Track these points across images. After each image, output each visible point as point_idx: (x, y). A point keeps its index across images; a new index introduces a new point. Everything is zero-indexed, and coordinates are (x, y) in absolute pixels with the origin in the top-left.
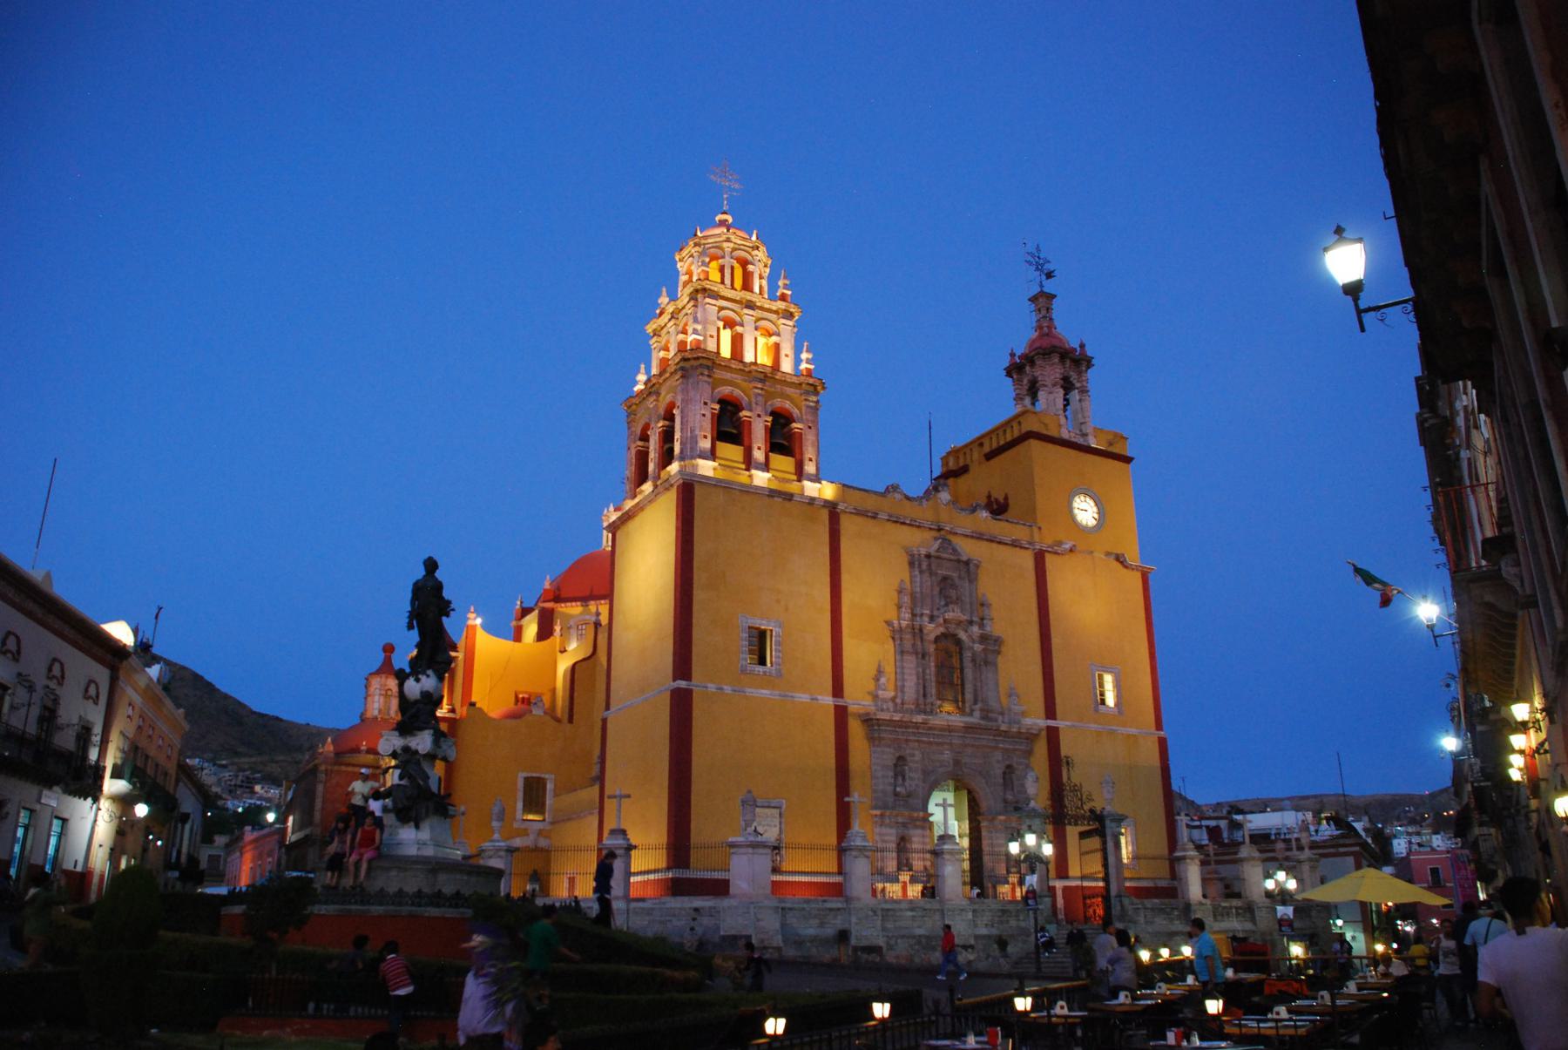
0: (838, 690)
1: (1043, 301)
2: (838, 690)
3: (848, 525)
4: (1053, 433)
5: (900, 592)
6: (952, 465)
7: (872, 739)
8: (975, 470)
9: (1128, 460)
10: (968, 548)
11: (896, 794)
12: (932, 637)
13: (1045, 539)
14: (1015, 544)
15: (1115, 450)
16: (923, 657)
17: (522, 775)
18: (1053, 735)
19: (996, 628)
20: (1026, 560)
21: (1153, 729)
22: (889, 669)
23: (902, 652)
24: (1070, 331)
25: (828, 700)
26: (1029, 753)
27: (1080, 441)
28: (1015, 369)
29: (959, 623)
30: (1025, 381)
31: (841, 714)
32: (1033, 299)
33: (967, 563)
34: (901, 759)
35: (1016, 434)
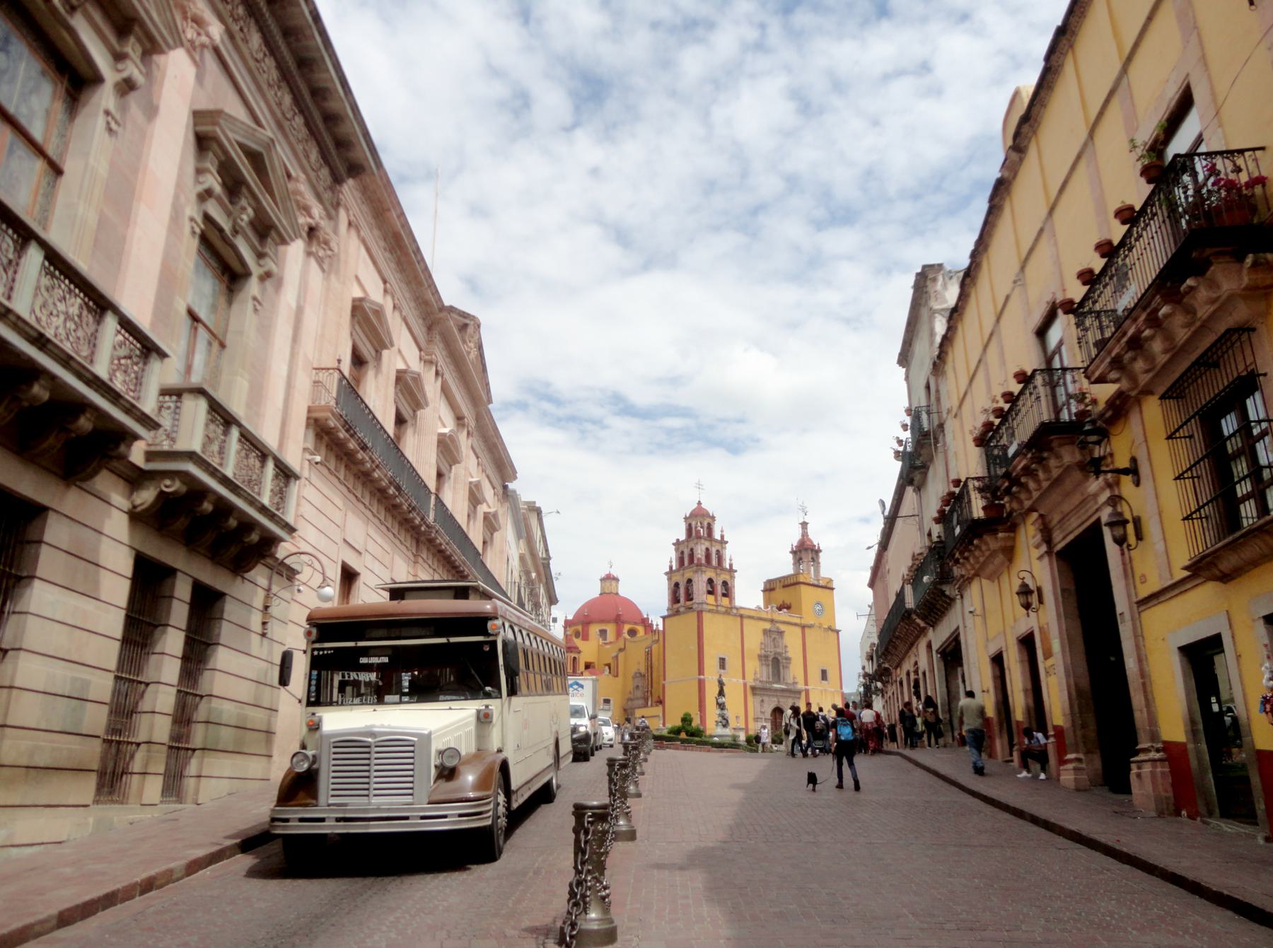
0: (744, 677)
1: (804, 525)
2: (744, 677)
3: (746, 621)
4: (808, 581)
5: (762, 643)
6: (768, 587)
7: (754, 694)
8: (777, 590)
9: (833, 589)
10: (782, 627)
11: (762, 712)
12: (770, 659)
13: (804, 622)
14: (796, 625)
15: (829, 585)
16: (768, 665)
17: (603, 698)
18: (807, 692)
19: (790, 655)
20: (798, 630)
21: (839, 689)
22: (758, 670)
23: (762, 664)
24: (815, 538)
25: (741, 681)
26: (799, 698)
27: (816, 583)
28: (794, 552)
29: (780, 654)
30: (798, 557)
31: (745, 685)
32: (801, 524)
33: (781, 633)
34: (762, 701)
35: (795, 581)
